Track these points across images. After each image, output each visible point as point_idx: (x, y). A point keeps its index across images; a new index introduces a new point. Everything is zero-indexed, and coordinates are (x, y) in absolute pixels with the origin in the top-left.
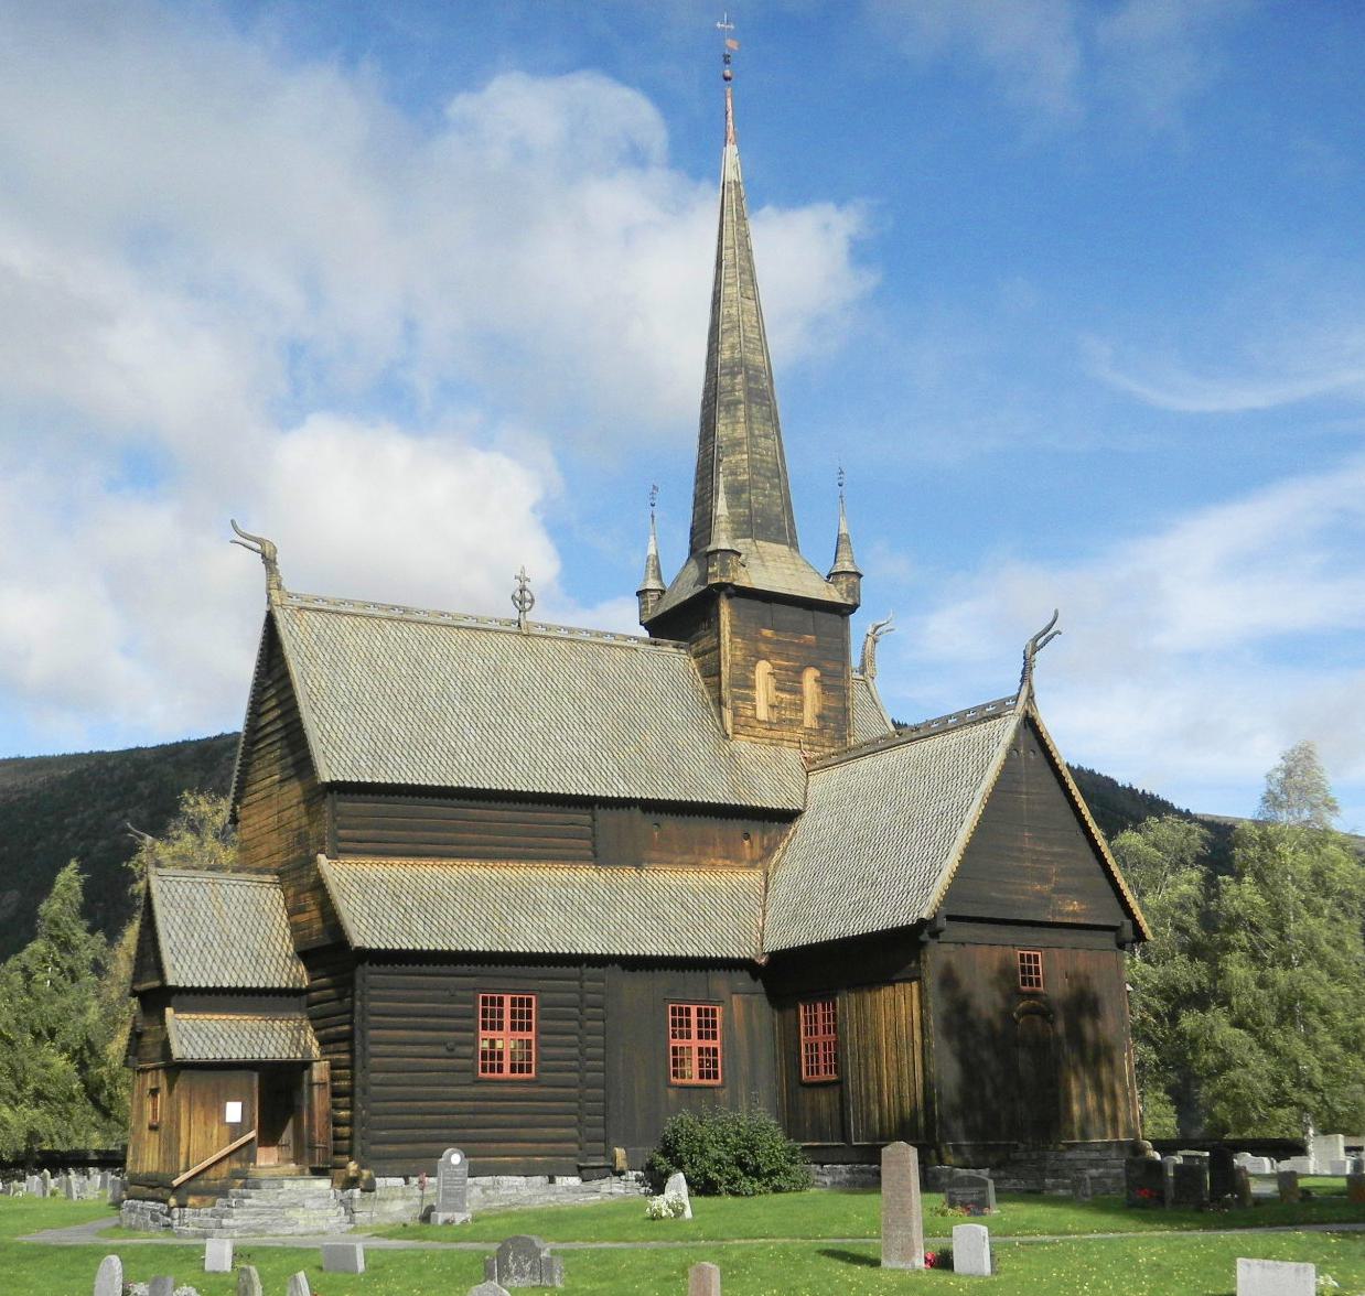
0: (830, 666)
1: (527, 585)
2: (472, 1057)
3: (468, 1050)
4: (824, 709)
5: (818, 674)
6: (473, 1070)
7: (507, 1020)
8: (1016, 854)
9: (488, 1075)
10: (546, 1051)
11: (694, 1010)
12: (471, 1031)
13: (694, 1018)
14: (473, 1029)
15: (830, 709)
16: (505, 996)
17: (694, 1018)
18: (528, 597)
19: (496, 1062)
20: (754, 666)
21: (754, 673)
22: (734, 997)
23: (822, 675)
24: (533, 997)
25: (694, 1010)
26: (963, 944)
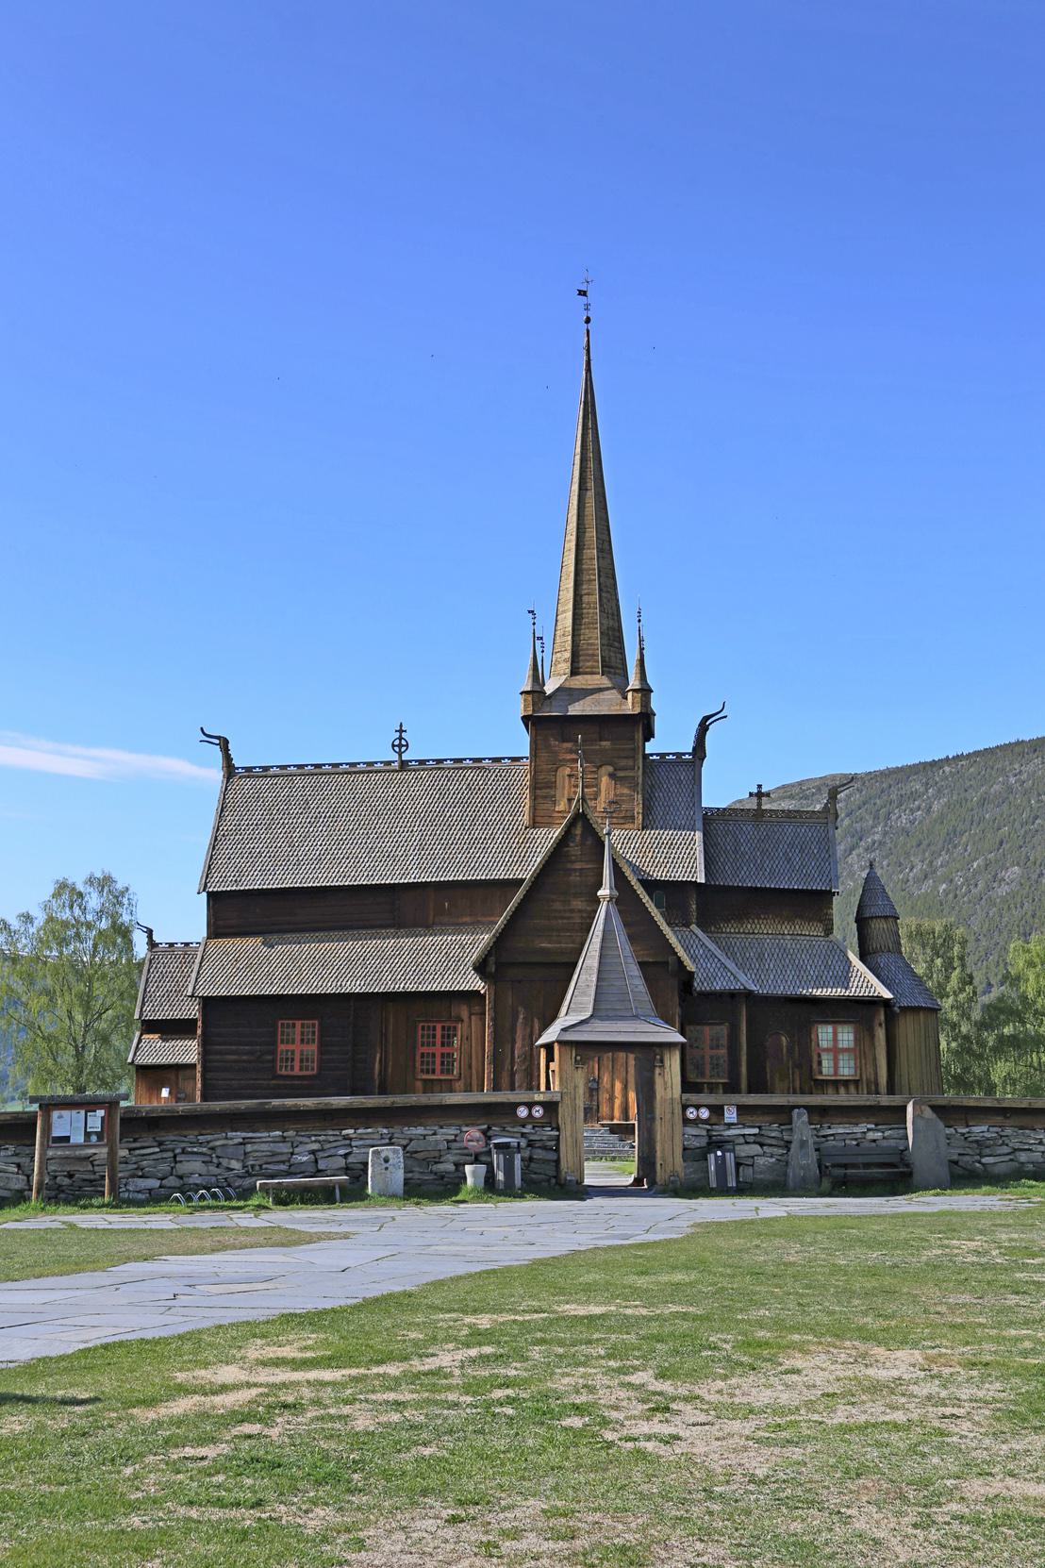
0: (623, 763)
1: (403, 735)
2: (274, 1061)
3: (270, 1057)
4: (616, 795)
5: (610, 769)
6: (273, 1069)
7: (298, 1038)
8: (568, 915)
9: (283, 1072)
10: (324, 1057)
11: (439, 1027)
12: (273, 1045)
13: (439, 1032)
14: (274, 1043)
15: (622, 795)
16: (296, 1022)
17: (439, 1032)
18: (403, 742)
19: (289, 1064)
20: (556, 771)
21: (555, 775)
22: (473, 1017)
23: (615, 770)
24: (316, 1022)
25: (439, 1027)
26: (520, 982)
